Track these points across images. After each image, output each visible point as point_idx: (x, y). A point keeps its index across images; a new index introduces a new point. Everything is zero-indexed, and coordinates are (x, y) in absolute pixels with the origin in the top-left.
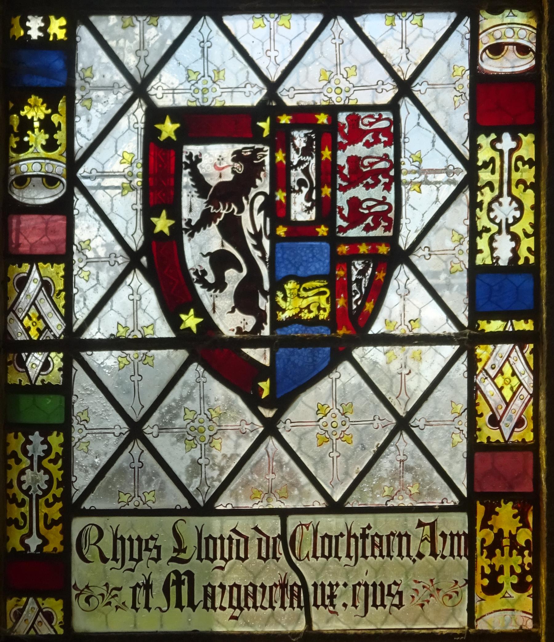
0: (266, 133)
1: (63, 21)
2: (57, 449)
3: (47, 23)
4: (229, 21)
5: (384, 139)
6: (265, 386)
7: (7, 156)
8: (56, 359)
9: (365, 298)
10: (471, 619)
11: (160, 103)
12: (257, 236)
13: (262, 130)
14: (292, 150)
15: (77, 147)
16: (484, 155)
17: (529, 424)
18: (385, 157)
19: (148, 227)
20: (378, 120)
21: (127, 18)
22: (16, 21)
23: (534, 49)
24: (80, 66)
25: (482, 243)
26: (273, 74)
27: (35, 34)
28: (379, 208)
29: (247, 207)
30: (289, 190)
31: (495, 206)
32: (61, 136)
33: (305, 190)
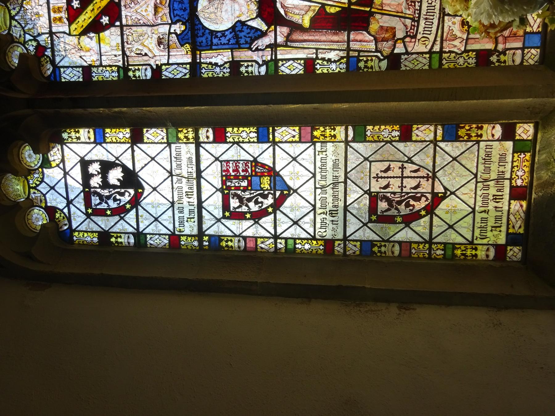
0: (228, 191)
1: (204, 237)
2: (300, 241)
3: (205, 241)
4: (203, 200)
5: (228, 164)
6: (285, 192)
7: (234, 250)
8: (279, 241)
9: (265, 168)
10: (342, 142)
11: (222, 216)
12: (251, 194)
13: (227, 192)
14: (231, 185)
15: (231, 235)
16: (231, 140)
17: (295, 128)
18: (233, 163)
19: (249, 219)
20: (224, 165)
21: (203, 223)
22: (205, 248)
23: (207, 129)
24: (214, 234)
25: (252, 140)
26: (215, 190)
27: (207, 244)
28: (244, 165)
29: (244, 196)
30: (240, 186)
31: (243, 137)
32: (229, 238)
33: (240, 182)
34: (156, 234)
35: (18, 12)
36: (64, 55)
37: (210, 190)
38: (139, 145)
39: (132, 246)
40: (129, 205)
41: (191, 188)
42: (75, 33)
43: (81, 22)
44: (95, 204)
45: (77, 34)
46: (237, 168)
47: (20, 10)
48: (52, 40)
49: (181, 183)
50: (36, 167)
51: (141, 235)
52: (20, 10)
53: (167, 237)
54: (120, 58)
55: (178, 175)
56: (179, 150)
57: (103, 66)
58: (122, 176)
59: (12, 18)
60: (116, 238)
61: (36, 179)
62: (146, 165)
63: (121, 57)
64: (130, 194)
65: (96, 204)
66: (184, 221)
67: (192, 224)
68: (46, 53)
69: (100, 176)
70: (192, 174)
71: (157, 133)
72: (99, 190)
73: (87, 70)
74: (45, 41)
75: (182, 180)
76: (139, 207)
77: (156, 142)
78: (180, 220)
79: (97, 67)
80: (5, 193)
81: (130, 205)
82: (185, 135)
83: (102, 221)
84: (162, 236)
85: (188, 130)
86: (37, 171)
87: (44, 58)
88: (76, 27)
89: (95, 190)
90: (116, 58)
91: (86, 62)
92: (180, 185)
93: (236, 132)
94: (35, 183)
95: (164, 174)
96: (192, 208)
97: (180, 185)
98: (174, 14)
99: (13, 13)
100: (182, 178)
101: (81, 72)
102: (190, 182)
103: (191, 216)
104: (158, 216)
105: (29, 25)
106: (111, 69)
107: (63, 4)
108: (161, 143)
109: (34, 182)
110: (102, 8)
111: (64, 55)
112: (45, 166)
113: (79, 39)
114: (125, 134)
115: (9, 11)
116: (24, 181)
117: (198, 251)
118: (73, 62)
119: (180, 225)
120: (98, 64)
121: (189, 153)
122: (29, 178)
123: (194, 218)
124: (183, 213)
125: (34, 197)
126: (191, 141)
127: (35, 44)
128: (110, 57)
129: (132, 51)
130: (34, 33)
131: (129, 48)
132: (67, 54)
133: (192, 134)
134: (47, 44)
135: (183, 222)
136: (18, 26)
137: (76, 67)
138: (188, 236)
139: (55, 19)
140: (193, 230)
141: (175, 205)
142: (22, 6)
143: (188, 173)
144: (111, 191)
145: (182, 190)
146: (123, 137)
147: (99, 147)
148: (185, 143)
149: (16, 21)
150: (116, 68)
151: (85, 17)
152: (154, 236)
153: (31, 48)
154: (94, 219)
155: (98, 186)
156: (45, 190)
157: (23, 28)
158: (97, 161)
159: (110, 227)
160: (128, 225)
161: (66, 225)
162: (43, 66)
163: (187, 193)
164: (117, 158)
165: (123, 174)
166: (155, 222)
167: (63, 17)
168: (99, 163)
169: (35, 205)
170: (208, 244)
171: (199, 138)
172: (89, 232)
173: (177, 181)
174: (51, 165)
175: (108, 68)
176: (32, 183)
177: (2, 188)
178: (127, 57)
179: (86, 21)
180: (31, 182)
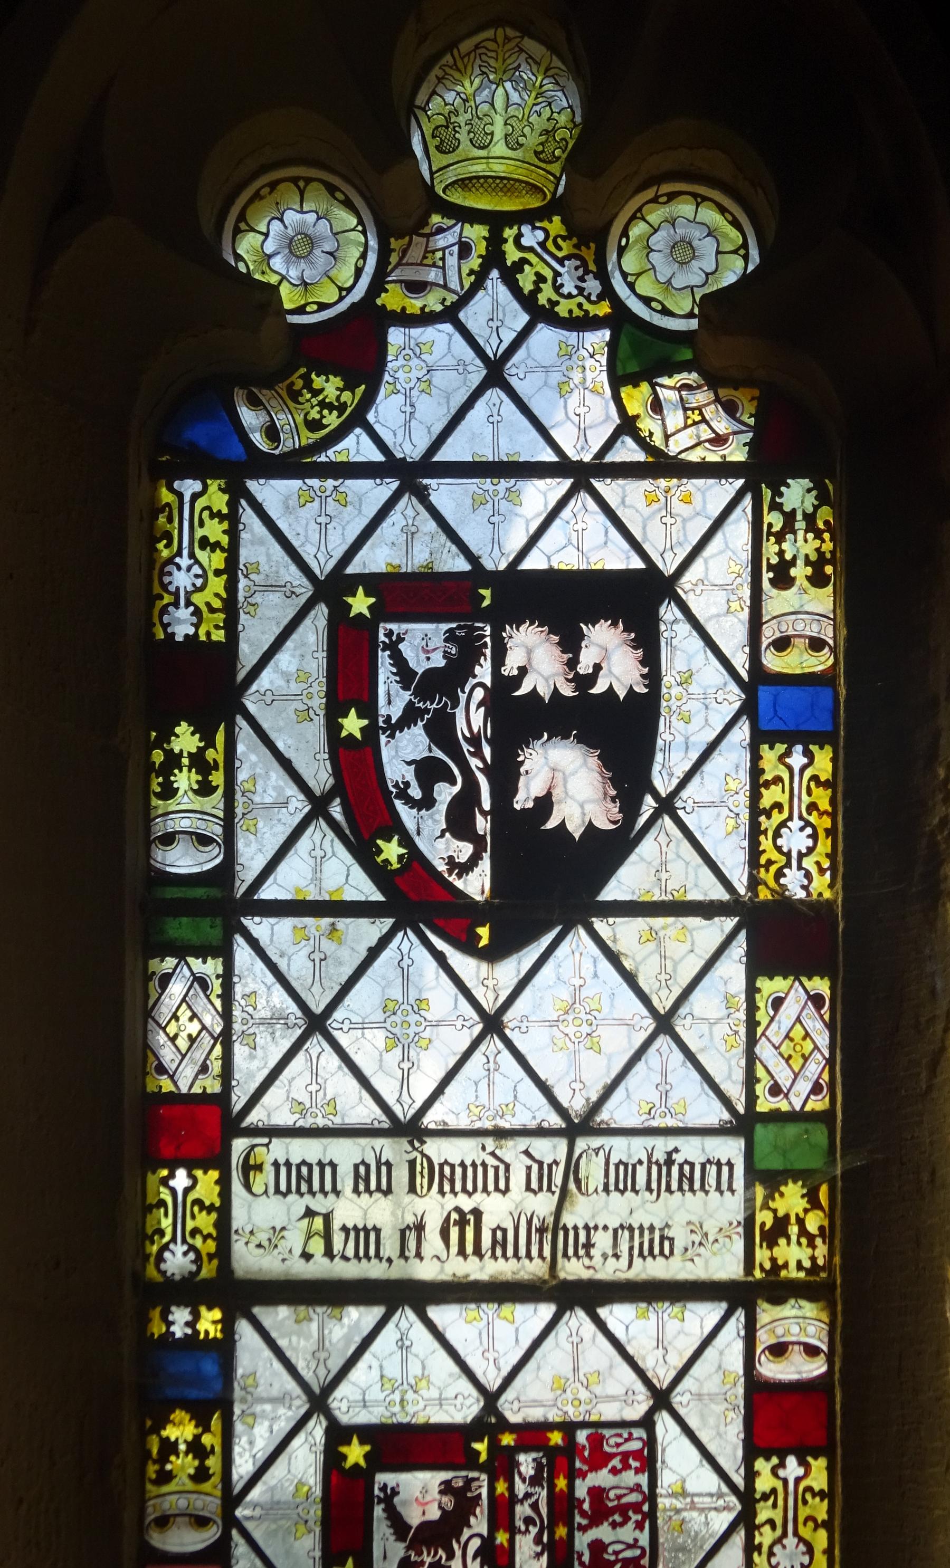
0: (483, 1457)
1: (217, 1314)
3: (196, 1316)
4: (434, 1313)
5: (635, 1464)
7: (143, 1491)
11: (345, 1419)
13: (478, 1453)
14: (517, 1478)
15: (235, 1477)
16: (764, 1483)
18: (637, 1488)
20: (626, 1440)
21: (302, 1309)
22: (156, 1314)
23: (825, 1348)
24: (240, 1372)
26: (492, 1381)
27: (179, 1331)
28: (628, 1554)
29: (458, 1553)
30: (513, 1531)
31: (777, 1549)
32: (213, 1463)
33: (534, 1530)
34: (227, 1015)
37: (491, 1355)
38: (739, 948)
39: (148, 856)
40: (400, 857)
41: (500, 1243)
44: (400, 639)
46: (613, 1511)
49: (528, 1188)
50: (618, 284)
51: (218, 921)
53: (214, 1087)
55: (572, 1167)
56: (712, 1180)
58: (570, 827)
60: (199, 762)
61: (549, 274)
62: (630, 978)
64: (465, 869)
65: (401, 646)
66: (311, 1191)
67: (295, 1240)
69: (567, 691)
70: (581, 1252)
71: (806, 1059)
72: (484, 672)
75: (543, 1196)
76: (388, 922)
77: (757, 1050)
78: (316, 1171)
80: (466, 46)
81: (396, 866)
82: (793, 1219)
83: (301, 675)
84: (218, 1049)
85: (819, 1241)
86: (593, 286)
89: (488, 652)
92: (518, 1178)
93: (803, 1512)
94: (524, 261)
95: (577, 1086)
96: (390, 1247)
97: (518, 1178)
100: (558, 1191)
102: (535, 1237)
103: (338, 1240)
104: (336, 1034)
108: (751, 1080)
109: (531, 257)
112: (624, 346)
114: (800, 867)
116: (535, 189)
117: (138, 1277)
119: (283, 1171)
121: (697, 1238)
122: (556, 226)
123: (329, 1253)
124: (356, 1190)
125: (441, 241)
126: (762, 1255)
133: (799, 1263)
135: (304, 1188)
138: (224, 1212)
140: (259, 1246)
141: (404, 1143)
143: (587, 1227)
144: (478, 754)
145: (491, 1187)
146: (788, 855)
147: (734, 697)
148: (749, 1222)
152: (218, 1003)
154: (307, 622)
155: (510, 667)
156: (483, 320)
158: (654, 677)
159: (265, 726)
160: (281, 839)
161: (272, 433)
163: (471, 1218)
164: (667, 806)
165: (577, 836)
166: (299, 1014)
168: (641, 689)
169: (394, 243)
170: (179, 1335)
171: (777, 1300)
172: (231, 586)
173: (540, 1164)
174: (634, 380)
176: (525, 242)
177: (489, 33)
180: (531, 238)
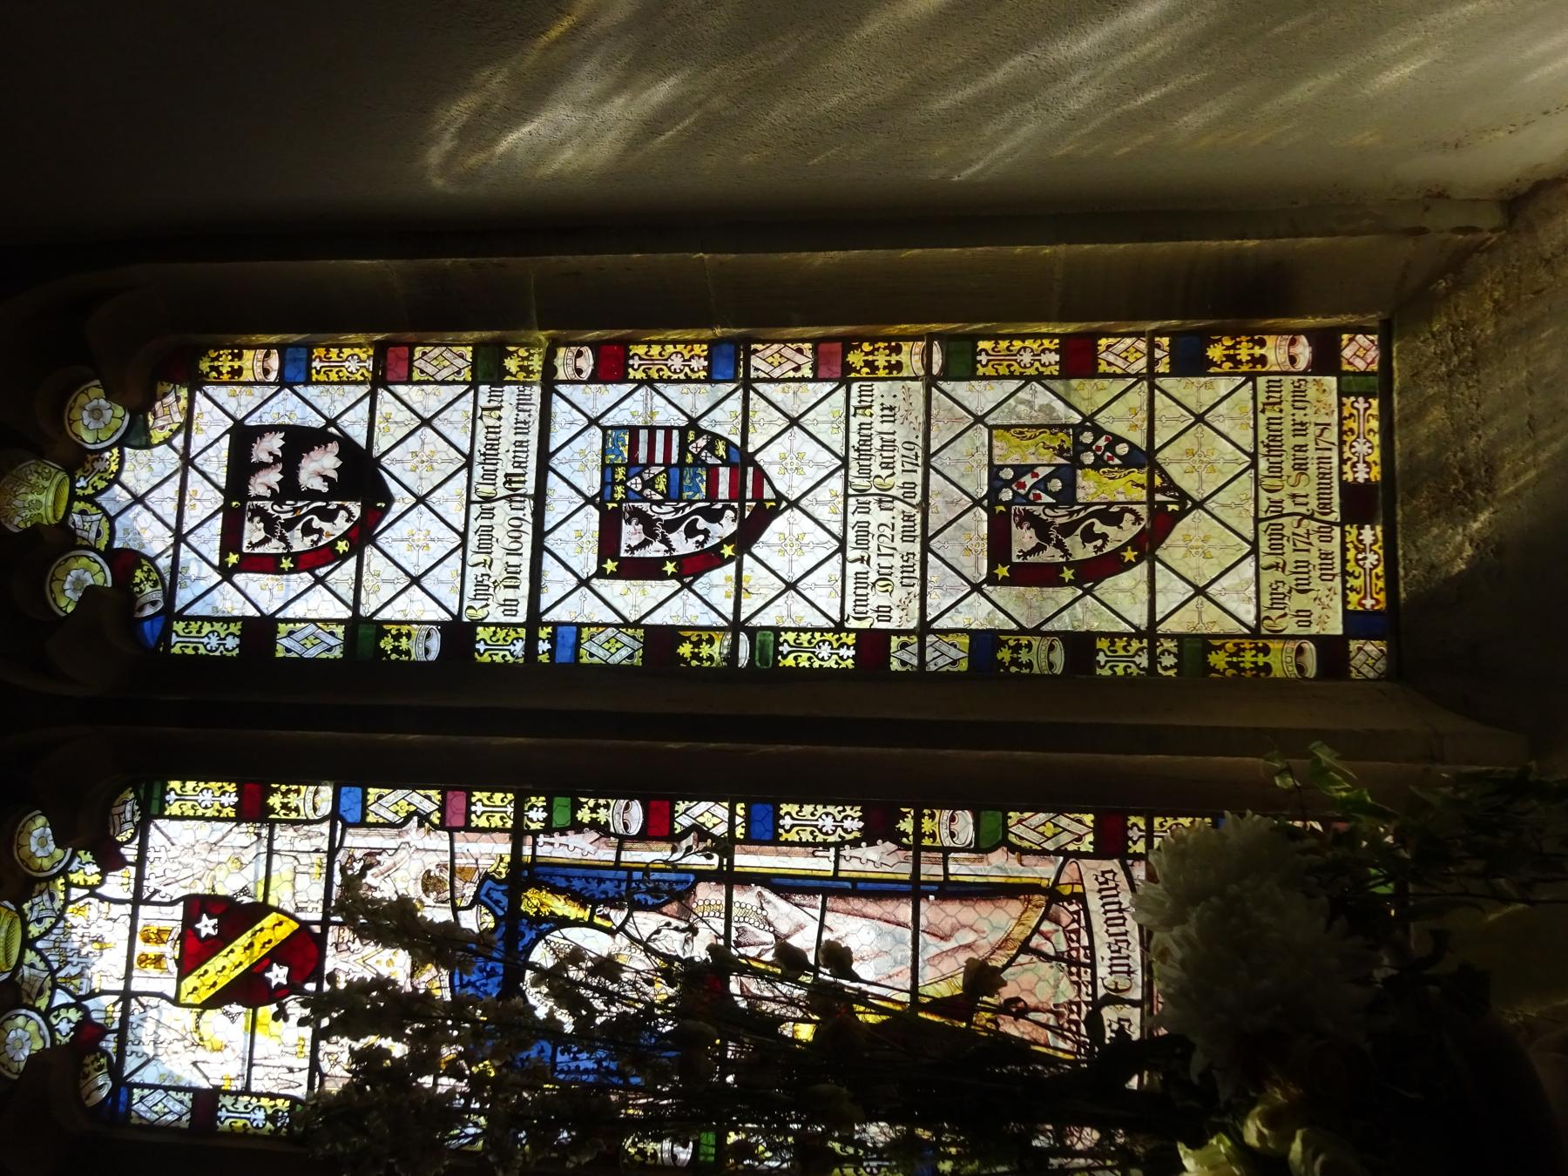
35: (48, 931)
36: (151, 1054)
42: (191, 999)
43: (212, 972)
45: (199, 1002)
47: (54, 926)
48: (126, 1012)
52: (54, 926)
54: (303, 1077)
57: (252, 1095)
59: (28, 943)
63: (306, 1073)
68: (103, 1044)
73: (206, 1101)
74: (106, 1011)
79: (237, 1094)
87: (92, 1058)
88: (197, 983)
90: (290, 1076)
91: (208, 1079)
98: (461, 979)
99: (35, 930)
101: (190, 1105)
105: (69, 967)
106: (272, 1103)
107: (174, 924)
110: (274, 944)
111: (151, 1054)
113: (199, 1016)
115: (25, 925)
118: (170, 1075)
120: (239, 1088)
127: (74, 1015)
128: (275, 1073)
129: (337, 1062)
130: (80, 989)
131: (330, 1054)
132: (160, 1051)
134: (109, 1021)
136: (41, 965)
137: (178, 1089)
139: (144, 959)
142: (60, 916)
149: (39, 952)
150: (288, 1103)
151: (225, 962)
153: (64, 1027)
157: (53, 973)
162: (87, 1076)
167: (167, 955)
175: (265, 1102)
178: (323, 1076)
179: (226, 972)
